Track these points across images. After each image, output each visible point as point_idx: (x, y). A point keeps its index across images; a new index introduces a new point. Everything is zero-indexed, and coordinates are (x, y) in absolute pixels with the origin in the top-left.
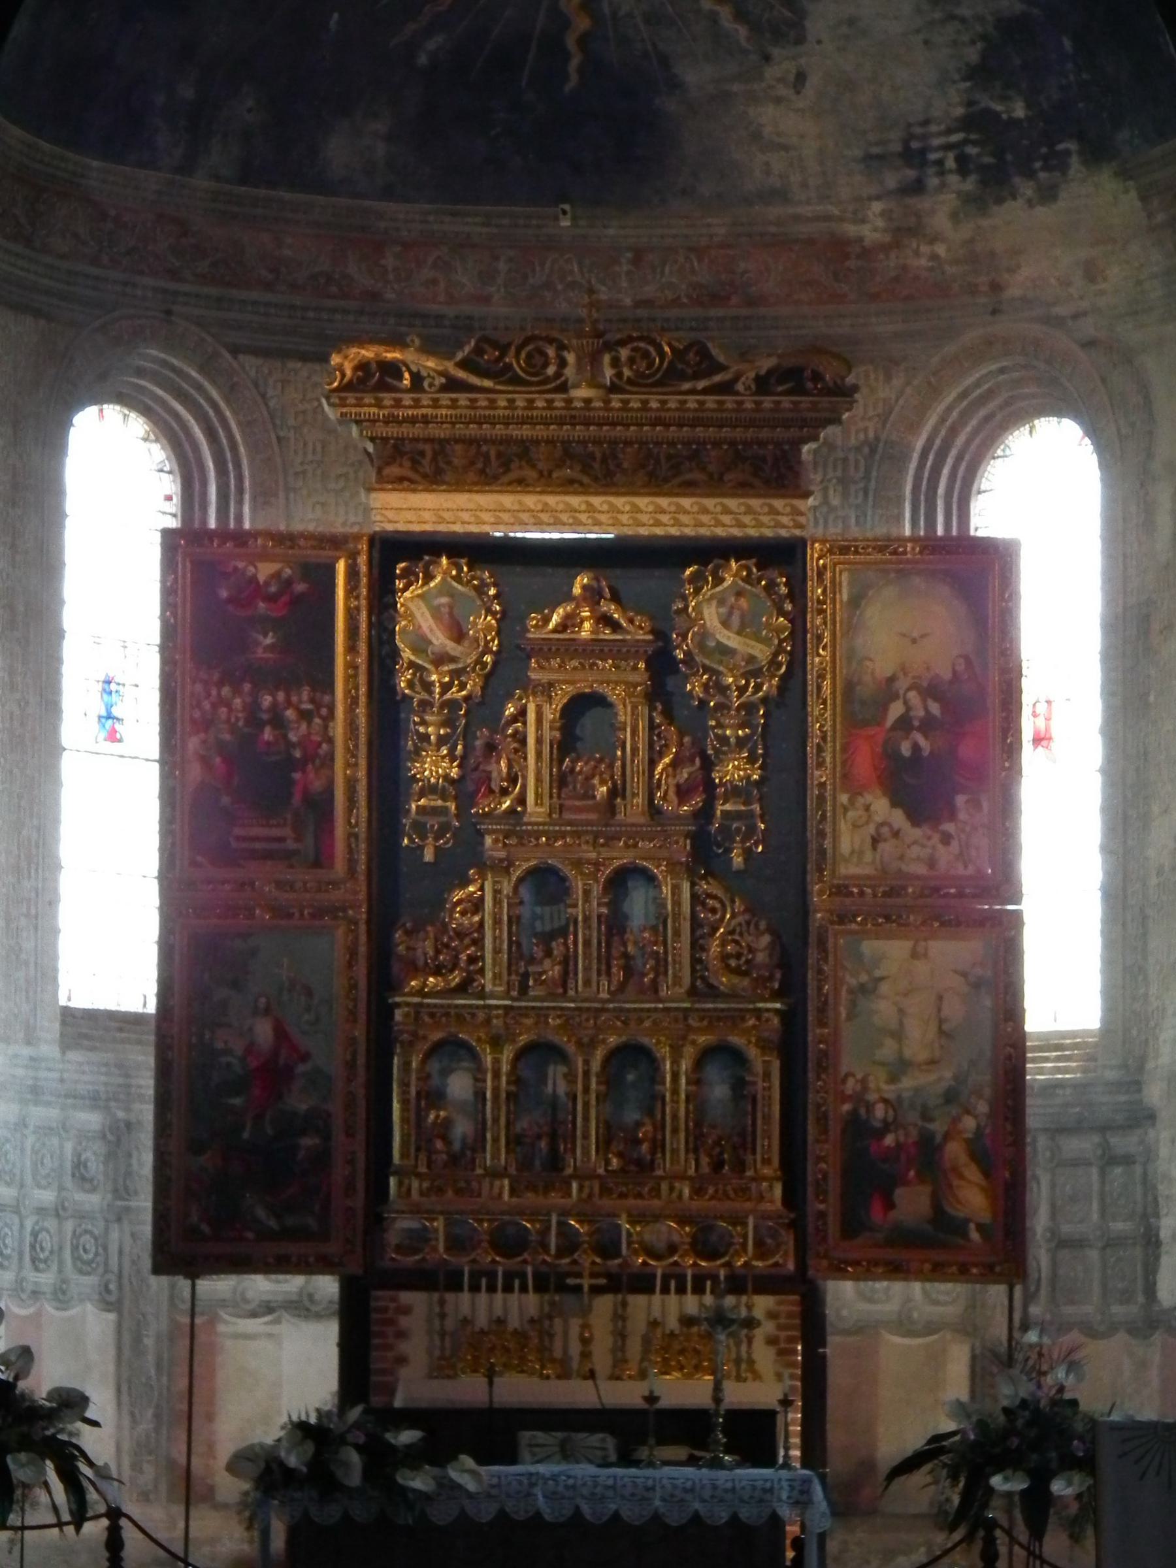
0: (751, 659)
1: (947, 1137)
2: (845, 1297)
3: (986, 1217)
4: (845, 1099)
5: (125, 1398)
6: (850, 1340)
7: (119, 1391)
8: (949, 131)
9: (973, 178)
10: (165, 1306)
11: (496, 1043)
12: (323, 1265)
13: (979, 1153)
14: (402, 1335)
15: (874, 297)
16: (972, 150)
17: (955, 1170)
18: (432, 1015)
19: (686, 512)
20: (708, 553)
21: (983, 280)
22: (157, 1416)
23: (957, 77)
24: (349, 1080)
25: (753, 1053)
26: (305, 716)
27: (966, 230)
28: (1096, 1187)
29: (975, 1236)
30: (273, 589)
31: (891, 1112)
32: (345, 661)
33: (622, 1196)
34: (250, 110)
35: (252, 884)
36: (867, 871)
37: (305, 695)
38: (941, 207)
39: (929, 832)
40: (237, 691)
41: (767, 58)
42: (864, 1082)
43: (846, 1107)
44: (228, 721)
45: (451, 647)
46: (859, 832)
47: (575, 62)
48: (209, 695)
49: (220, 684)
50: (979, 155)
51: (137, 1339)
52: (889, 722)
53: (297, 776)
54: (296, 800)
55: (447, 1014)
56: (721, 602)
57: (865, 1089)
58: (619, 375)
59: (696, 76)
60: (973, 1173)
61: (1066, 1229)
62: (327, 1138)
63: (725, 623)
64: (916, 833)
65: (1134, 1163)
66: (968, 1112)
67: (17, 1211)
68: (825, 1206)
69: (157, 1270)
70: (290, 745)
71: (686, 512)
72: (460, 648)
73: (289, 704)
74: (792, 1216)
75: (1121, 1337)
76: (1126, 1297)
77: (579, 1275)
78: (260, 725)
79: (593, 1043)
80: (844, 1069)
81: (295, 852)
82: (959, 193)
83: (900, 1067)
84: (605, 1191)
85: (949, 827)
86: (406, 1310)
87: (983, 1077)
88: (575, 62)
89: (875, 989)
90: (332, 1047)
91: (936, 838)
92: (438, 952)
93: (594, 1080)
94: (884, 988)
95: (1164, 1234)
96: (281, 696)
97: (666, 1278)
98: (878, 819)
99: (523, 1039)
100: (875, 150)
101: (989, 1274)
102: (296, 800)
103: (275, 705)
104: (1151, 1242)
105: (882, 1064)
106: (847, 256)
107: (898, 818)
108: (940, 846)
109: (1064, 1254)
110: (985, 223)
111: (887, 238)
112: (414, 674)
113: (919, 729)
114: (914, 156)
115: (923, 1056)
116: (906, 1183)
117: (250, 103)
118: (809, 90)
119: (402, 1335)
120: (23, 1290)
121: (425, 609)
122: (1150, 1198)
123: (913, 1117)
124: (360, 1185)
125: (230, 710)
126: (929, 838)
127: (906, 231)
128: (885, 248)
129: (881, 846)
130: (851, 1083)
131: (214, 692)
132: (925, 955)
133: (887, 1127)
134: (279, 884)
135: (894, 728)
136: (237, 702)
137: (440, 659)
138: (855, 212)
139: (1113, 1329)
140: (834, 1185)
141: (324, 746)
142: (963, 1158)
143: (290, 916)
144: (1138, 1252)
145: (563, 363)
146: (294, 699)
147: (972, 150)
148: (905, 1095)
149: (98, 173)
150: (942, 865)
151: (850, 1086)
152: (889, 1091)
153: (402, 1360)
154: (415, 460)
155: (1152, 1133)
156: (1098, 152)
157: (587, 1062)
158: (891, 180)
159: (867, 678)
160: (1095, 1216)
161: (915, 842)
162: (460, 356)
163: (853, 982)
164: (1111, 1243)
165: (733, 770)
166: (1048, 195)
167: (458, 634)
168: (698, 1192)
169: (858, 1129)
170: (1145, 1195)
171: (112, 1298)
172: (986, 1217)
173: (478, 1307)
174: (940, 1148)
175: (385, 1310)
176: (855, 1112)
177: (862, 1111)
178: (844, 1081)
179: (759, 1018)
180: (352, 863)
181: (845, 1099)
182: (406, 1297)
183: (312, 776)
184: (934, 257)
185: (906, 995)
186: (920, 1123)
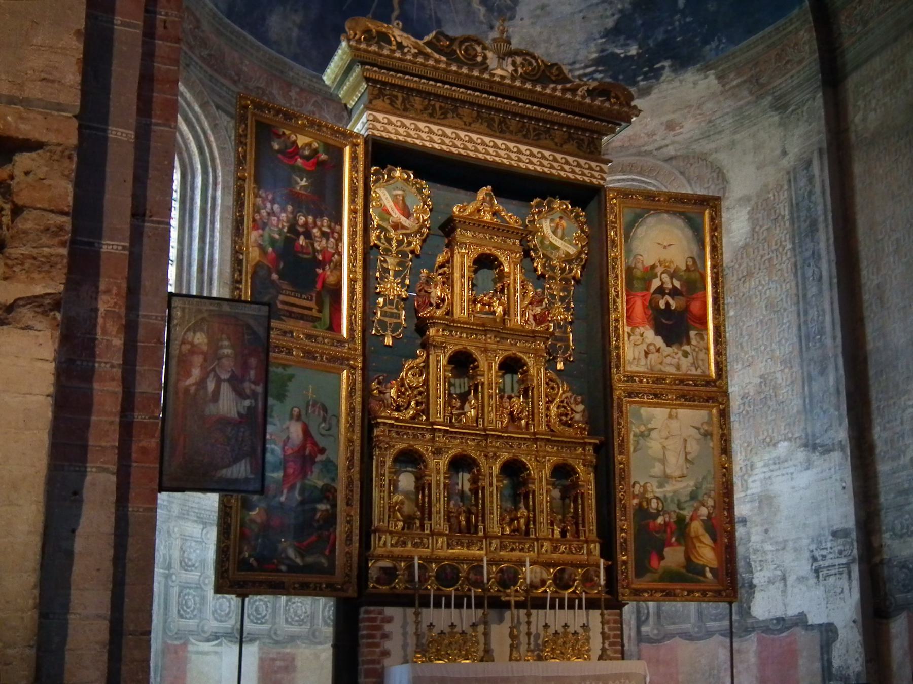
1: (692, 519)
4: (634, 496)
11: (438, 452)
14: (385, 636)
18: (398, 433)
24: (349, 469)
25: (580, 469)
31: (661, 504)
33: (513, 550)
35: (291, 332)
42: (644, 486)
43: (635, 501)
45: (403, 220)
53: (320, 271)
54: (318, 286)
55: (407, 434)
57: (645, 491)
58: (516, 71)
62: (334, 506)
66: (704, 505)
69: (219, 589)
72: (408, 222)
79: (496, 457)
83: (665, 479)
84: (503, 547)
86: (389, 620)
87: (710, 485)
89: (649, 435)
94: (654, 434)
99: (452, 453)
102: (318, 286)
105: (654, 477)
112: (381, 233)
115: (677, 473)
119: (385, 636)
124: (356, 538)
130: (637, 487)
132: (676, 417)
133: (658, 513)
134: (309, 337)
137: (397, 226)
140: (631, 546)
141: (336, 256)
143: (315, 358)
148: (669, 495)
151: (637, 490)
152: (659, 492)
153: (386, 653)
157: (491, 468)
163: (637, 431)
168: (555, 549)
169: (643, 514)
173: (440, 618)
177: (645, 504)
178: (633, 487)
179: (584, 449)
180: (351, 330)
182: (389, 611)
185: (667, 439)
186: (677, 510)
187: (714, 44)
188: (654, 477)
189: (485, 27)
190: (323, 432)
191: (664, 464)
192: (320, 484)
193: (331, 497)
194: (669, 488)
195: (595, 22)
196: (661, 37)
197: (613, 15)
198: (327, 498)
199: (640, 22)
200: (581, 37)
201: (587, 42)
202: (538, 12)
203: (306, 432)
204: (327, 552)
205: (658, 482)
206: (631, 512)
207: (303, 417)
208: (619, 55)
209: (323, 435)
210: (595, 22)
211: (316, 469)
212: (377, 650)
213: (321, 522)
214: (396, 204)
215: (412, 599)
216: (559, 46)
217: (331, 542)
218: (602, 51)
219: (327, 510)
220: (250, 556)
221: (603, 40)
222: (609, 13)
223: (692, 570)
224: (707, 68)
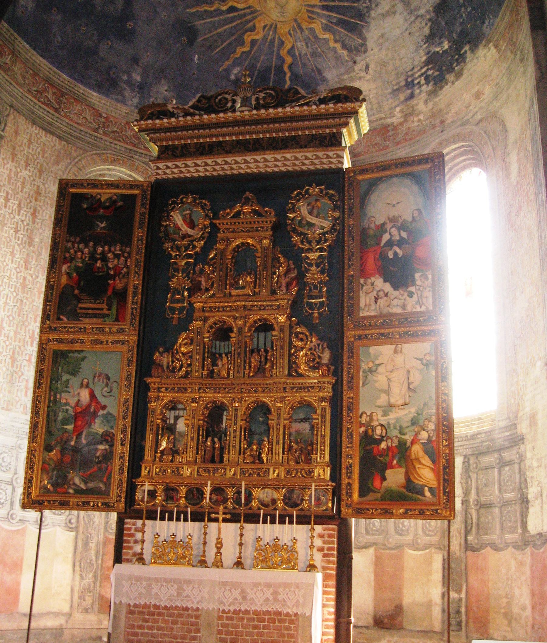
0: (323, 228)
1: (413, 443)
2: (357, 526)
3: (434, 484)
4: (361, 425)
5: (77, 568)
6: (393, 552)
7: (74, 565)
8: (421, 68)
9: (431, 84)
10: (102, 531)
12: (107, 507)
13: (431, 450)
15: (398, 143)
16: (430, 72)
17: (417, 459)
19: (288, 160)
21: (438, 121)
22: (95, 577)
23: (422, 43)
24: (124, 419)
26: (117, 256)
27: (430, 105)
28: (496, 478)
29: (428, 494)
30: (107, 204)
31: (384, 431)
34: (166, 91)
36: (373, 313)
37: (118, 248)
38: (421, 104)
39: (402, 292)
40: (86, 246)
41: (355, 62)
42: (371, 416)
43: (362, 429)
44: (81, 258)
45: (190, 231)
47: (288, 75)
48: (74, 247)
49: (79, 243)
50: (433, 74)
51: (86, 544)
52: (382, 245)
53: (111, 282)
54: (109, 293)
56: (309, 204)
57: (371, 419)
60: (426, 461)
61: (483, 499)
62: (111, 446)
63: (311, 213)
64: (396, 293)
65: (514, 463)
66: (424, 430)
67: (12, 484)
70: (108, 268)
71: (288, 160)
73: (110, 251)
74: (334, 484)
75: (510, 549)
76: (513, 530)
77: (218, 513)
78: (96, 260)
80: (361, 411)
81: (108, 315)
82: (426, 92)
85: (412, 289)
88: (288, 75)
89: (377, 369)
91: (406, 294)
92: (173, 362)
93: (239, 419)
94: (381, 369)
95: (530, 497)
96: (106, 248)
97: (265, 516)
98: (378, 289)
100: (395, 88)
101: (435, 515)
103: (103, 251)
104: (525, 501)
105: (379, 407)
106: (388, 131)
107: (388, 287)
108: (408, 298)
109: (483, 511)
110: (436, 100)
111: (402, 120)
113: (397, 245)
114: (410, 84)
115: (401, 402)
116: (392, 467)
117: (166, 88)
118: (371, 71)
120: (13, 519)
121: (179, 216)
122: (523, 479)
123: (395, 433)
125: (83, 253)
126: (402, 295)
128: (401, 124)
129: (379, 301)
130: (364, 416)
131: (76, 246)
132: (401, 352)
135: (385, 245)
136: (86, 250)
138: (390, 114)
139: (507, 546)
141: (125, 269)
142: (421, 453)
144: (518, 507)
145: (234, 101)
146: (113, 249)
147: (430, 72)
148: (392, 422)
149: (94, 97)
150: (409, 308)
151: (364, 420)
152: (383, 420)
155: (522, 447)
156: (474, 47)
158: (402, 97)
159: (372, 226)
160: (497, 492)
161: (396, 298)
162: (191, 104)
163: (366, 368)
164: (506, 504)
165: (314, 275)
166: (459, 75)
167: (192, 225)
169: (368, 440)
170: (520, 478)
171: (73, 526)
172: (434, 484)
174: (409, 448)
175: (130, 529)
176: (366, 432)
177: (370, 431)
178: (361, 417)
181: (361, 425)
183: (118, 282)
184: (419, 120)
185: (391, 372)
186: (399, 435)
187: (487, 22)
188: (379, 407)
189: (351, 63)
190: (105, 394)
191: (388, 395)
192: (101, 431)
193: (109, 439)
194: (392, 416)
195: (417, 34)
196: (458, 29)
197: (426, 24)
198: (107, 441)
199: (443, 23)
200: (412, 48)
201: (417, 50)
202: (381, 40)
203: (92, 395)
204: (105, 480)
205: (384, 411)
206: (356, 439)
207: (91, 386)
208: (438, 52)
209: (105, 396)
210: (417, 34)
211: (98, 421)
212: (130, 551)
213: (101, 458)
214: (184, 221)
216: (401, 60)
217: (108, 472)
218: (428, 53)
219: (106, 449)
220: (48, 483)
221: (426, 45)
222: (423, 24)
223: (411, 487)
224: (488, 42)
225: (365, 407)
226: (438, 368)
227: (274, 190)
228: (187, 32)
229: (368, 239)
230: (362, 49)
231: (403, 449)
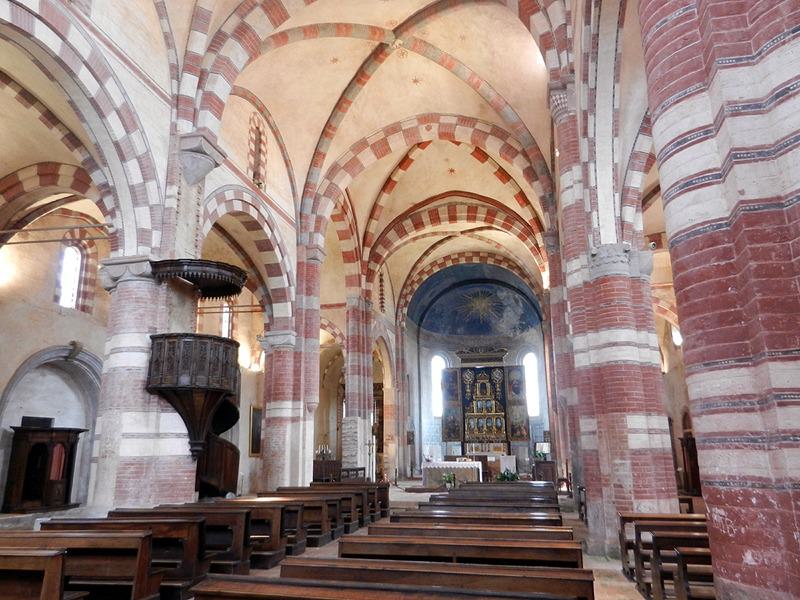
20: (494, 368)
32: (459, 381)
46: (510, 396)
59: (493, 322)
68: (510, 434)
90: (459, 419)
127: (515, 335)
149: (435, 334)
154: (463, 361)
169: (513, 426)
215: (469, 442)
223: (522, 435)
225: (511, 419)
226: (525, 410)
227: (489, 370)
228: (456, 313)
229: (511, 383)
230: (502, 317)
231: (520, 428)
